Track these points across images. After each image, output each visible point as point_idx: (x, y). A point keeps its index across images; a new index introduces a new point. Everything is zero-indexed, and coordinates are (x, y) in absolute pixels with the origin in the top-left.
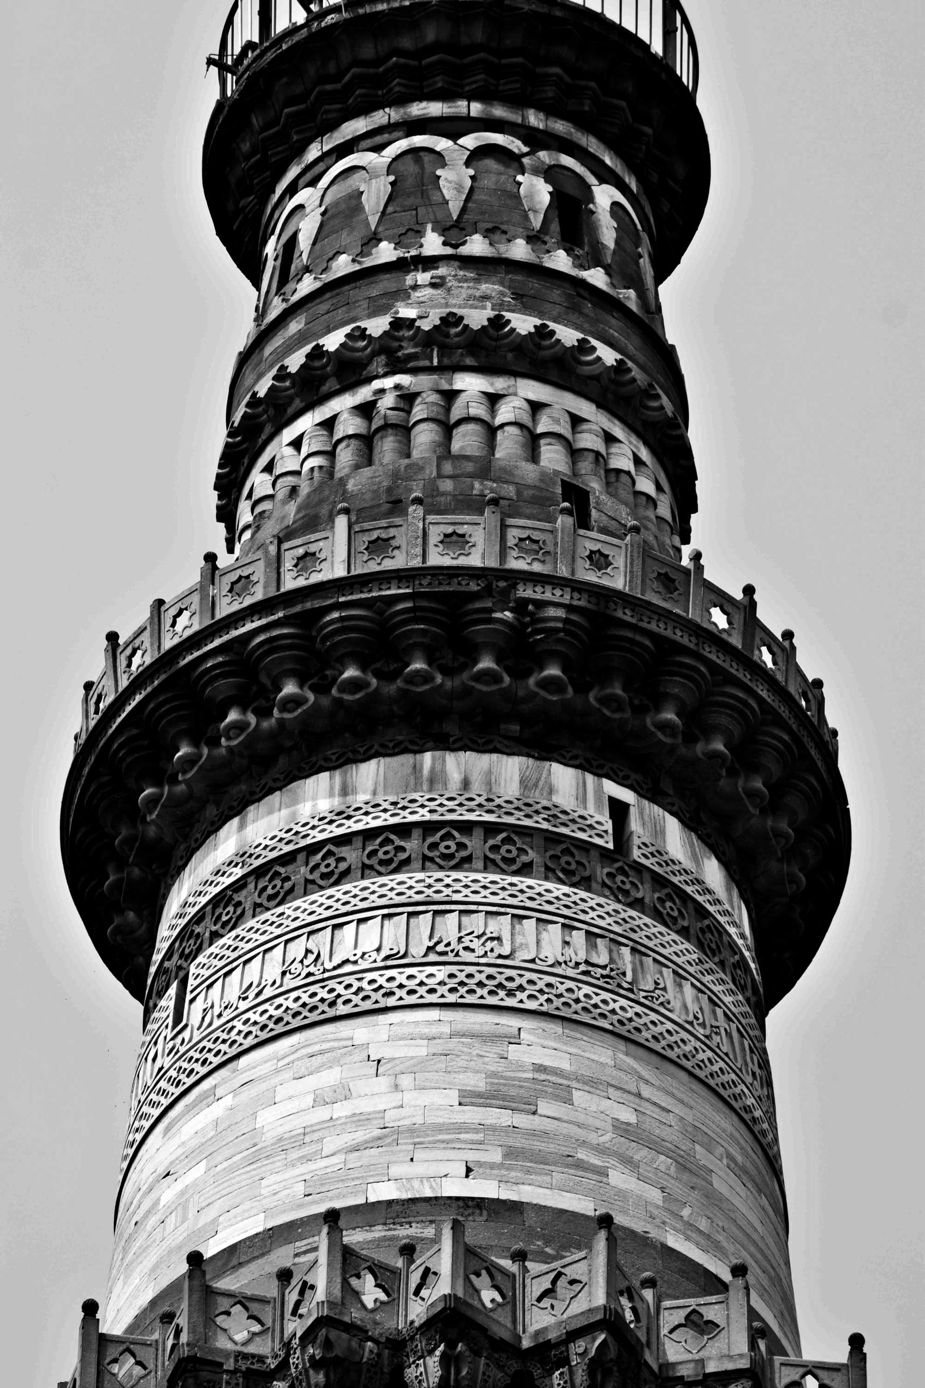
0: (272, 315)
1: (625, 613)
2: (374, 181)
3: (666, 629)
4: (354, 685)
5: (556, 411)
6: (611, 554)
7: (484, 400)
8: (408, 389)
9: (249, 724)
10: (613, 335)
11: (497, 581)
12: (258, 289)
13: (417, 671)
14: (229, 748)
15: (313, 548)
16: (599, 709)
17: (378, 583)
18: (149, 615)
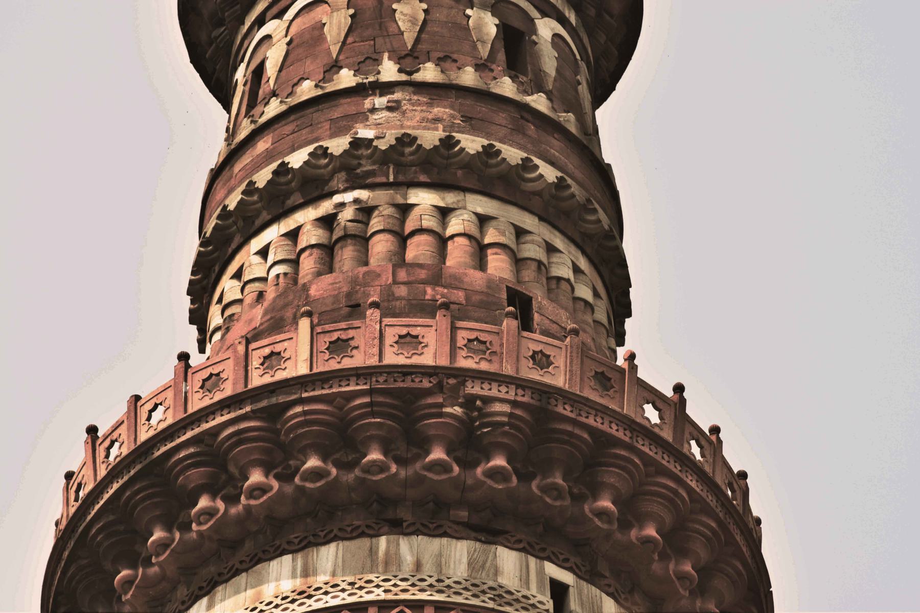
0: (242, 135)
1: (565, 409)
2: (335, 14)
3: (602, 424)
4: (316, 474)
5: (502, 223)
6: (552, 354)
7: (436, 214)
8: (366, 202)
9: (217, 510)
10: (554, 155)
11: (448, 378)
12: (229, 112)
13: (374, 462)
14: (198, 532)
15: (278, 348)
16: (541, 497)
17: (337, 380)
18: (126, 410)
